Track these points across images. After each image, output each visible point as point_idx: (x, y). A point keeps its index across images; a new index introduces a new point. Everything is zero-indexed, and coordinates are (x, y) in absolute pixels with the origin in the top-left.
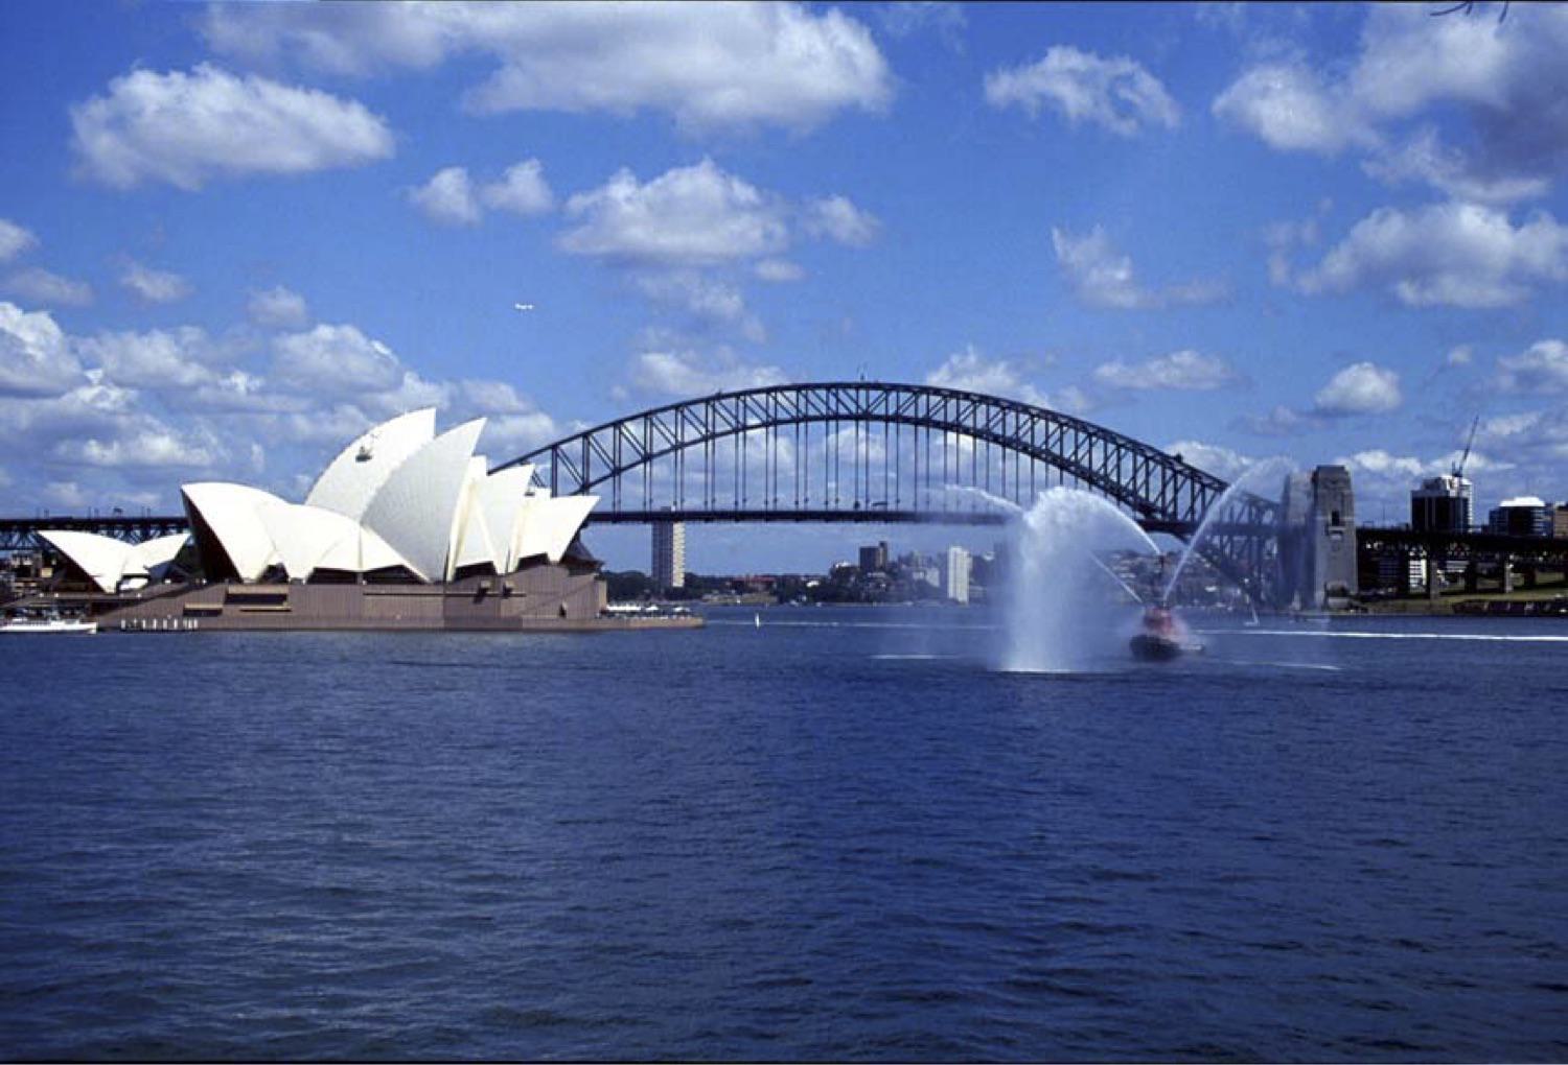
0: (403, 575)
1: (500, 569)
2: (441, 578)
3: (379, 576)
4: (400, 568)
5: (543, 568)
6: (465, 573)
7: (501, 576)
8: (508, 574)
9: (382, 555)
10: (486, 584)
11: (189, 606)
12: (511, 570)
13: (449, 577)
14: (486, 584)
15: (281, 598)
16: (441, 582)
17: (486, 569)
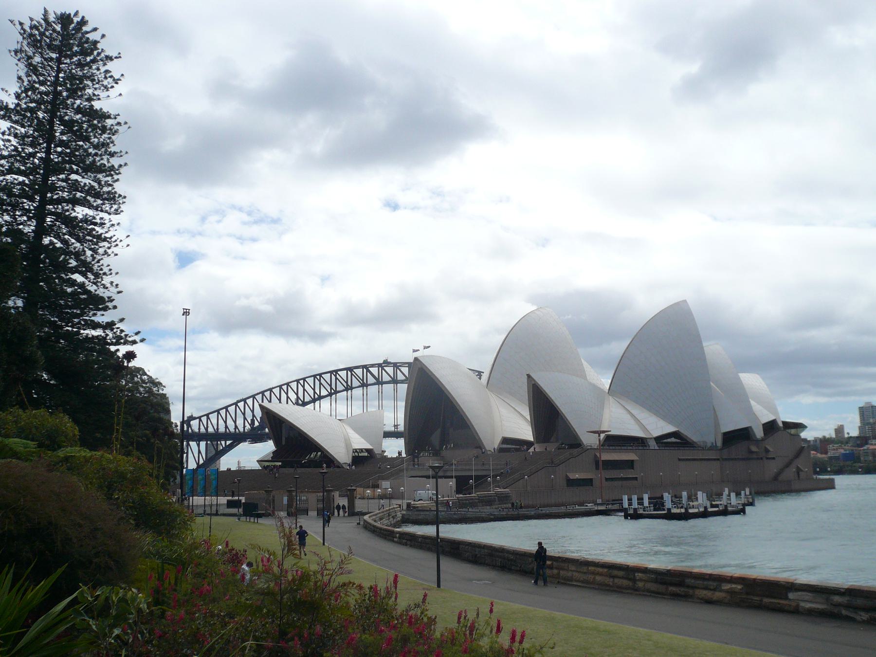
8: (763, 440)
10: (754, 448)
13: (719, 444)
15: (630, 464)
16: (713, 448)
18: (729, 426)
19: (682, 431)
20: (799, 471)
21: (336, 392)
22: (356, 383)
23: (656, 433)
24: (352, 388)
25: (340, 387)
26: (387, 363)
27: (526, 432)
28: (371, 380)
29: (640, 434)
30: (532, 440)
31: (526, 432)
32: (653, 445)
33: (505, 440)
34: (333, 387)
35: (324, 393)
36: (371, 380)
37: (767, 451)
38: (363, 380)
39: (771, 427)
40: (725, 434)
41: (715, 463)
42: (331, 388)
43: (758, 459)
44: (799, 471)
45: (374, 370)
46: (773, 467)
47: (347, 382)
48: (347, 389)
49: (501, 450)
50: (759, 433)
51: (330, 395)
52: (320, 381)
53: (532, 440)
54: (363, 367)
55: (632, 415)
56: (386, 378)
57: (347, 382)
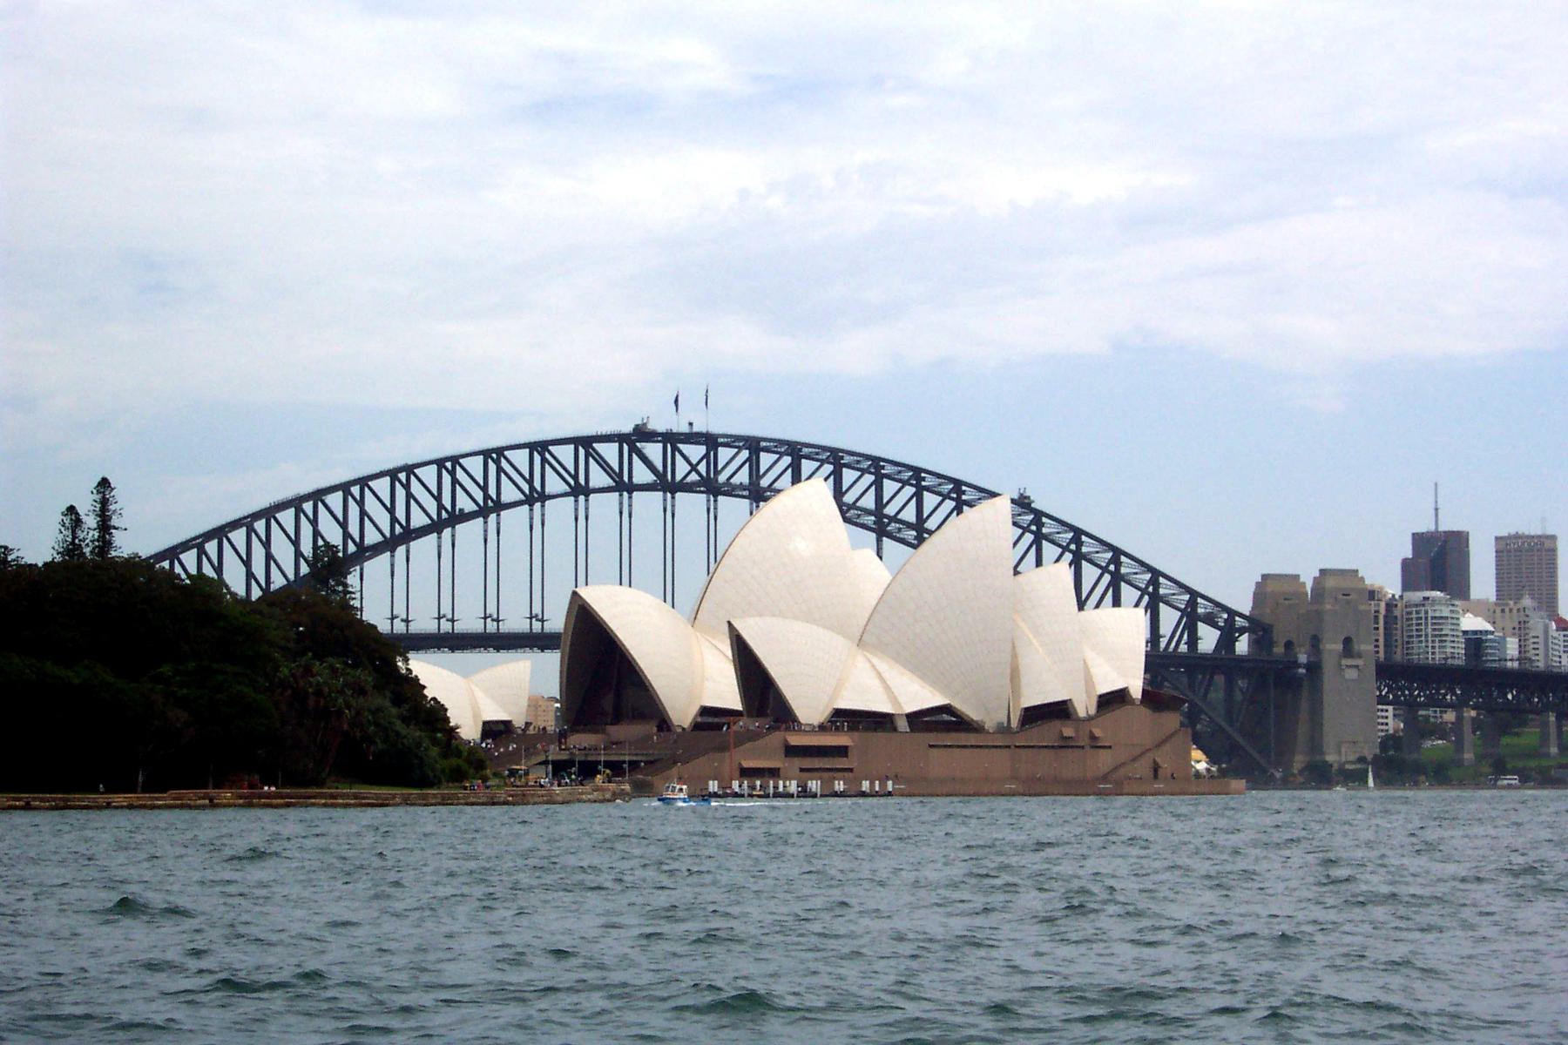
0: (946, 717)
8: (1090, 719)
9: (916, 695)
10: (1068, 732)
12: (1092, 711)
13: (1015, 723)
15: (842, 751)
16: (1004, 729)
17: (1059, 711)
18: (1034, 697)
19: (958, 705)
20: (1156, 769)
21: (499, 506)
22: (554, 484)
23: (909, 709)
24: (543, 497)
25: (509, 493)
26: (642, 434)
28: (599, 478)
29: (884, 707)
32: (903, 725)
33: (706, 711)
34: (492, 492)
35: (465, 504)
36: (599, 478)
37: (1093, 737)
38: (575, 477)
39: (1113, 700)
40: (1027, 710)
41: (1005, 751)
42: (487, 497)
44: (1156, 769)
45: (609, 451)
46: (1104, 760)
47: (530, 482)
48: (530, 500)
49: (696, 726)
50: (1084, 706)
51: (483, 512)
52: (452, 473)
54: (578, 441)
56: (642, 475)
57: (530, 482)
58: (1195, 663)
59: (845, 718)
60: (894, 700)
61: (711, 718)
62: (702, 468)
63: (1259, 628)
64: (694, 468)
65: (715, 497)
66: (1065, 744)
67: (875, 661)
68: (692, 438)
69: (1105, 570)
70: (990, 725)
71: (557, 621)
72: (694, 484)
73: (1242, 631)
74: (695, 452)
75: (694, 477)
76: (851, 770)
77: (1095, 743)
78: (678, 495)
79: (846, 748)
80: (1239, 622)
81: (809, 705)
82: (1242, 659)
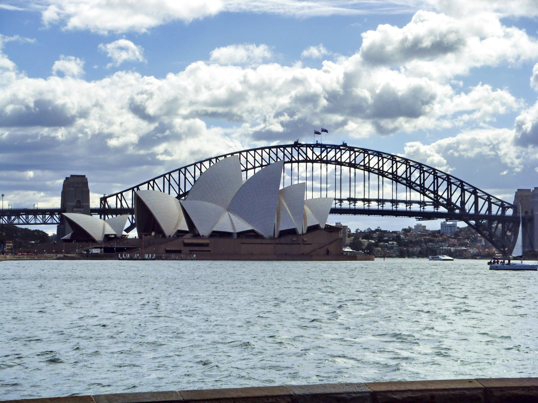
1: (300, 232)
2: (272, 234)
3: (241, 234)
4: (252, 231)
5: (318, 231)
6: (283, 233)
7: (300, 235)
8: (303, 234)
10: (294, 239)
11: (168, 249)
12: (305, 232)
13: (276, 236)
14: (294, 239)
15: (207, 245)
16: (273, 238)
17: (293, 232)
18: (283, 227)
23: (238, 230)
27: (184, 227)
29: (229, 230)
30: (188, 230)
31: (184, 227)
37: (303, 240)
40: (281, 231)
43: (297, 244)
53: (188, 230)
55: (231, 219)
58: (490, 217)
59: (216, 234)
60: (234, 228)
61: (180, 233)
62: (320, 157)
63: (511, 206)
64: (318, 157)
65: (327, 164)
66: (293, 243)
67: (231, 215)
68: (317, 145)
69: (458, 186)
70: (266, 236)
71: (128, 202)
72: (318, 160)
73: (508, 208)
74: (317, 151)
75: (318, 159)
76: (210, 251)
77: (305, 243)
78: (314, 164)
79: (208, 243)
80: (506, 205)
81: (204, 230)
82: (509, 217)
